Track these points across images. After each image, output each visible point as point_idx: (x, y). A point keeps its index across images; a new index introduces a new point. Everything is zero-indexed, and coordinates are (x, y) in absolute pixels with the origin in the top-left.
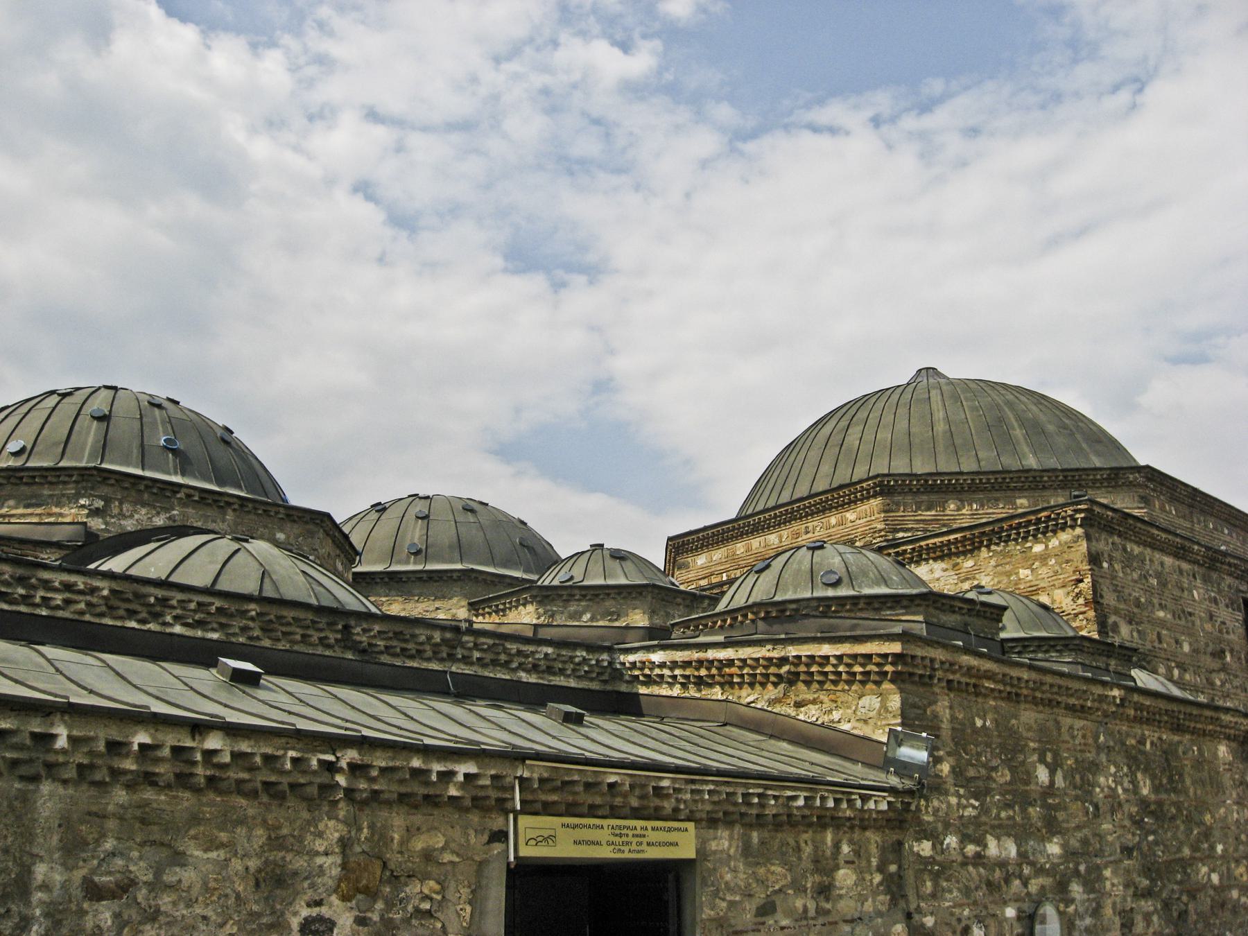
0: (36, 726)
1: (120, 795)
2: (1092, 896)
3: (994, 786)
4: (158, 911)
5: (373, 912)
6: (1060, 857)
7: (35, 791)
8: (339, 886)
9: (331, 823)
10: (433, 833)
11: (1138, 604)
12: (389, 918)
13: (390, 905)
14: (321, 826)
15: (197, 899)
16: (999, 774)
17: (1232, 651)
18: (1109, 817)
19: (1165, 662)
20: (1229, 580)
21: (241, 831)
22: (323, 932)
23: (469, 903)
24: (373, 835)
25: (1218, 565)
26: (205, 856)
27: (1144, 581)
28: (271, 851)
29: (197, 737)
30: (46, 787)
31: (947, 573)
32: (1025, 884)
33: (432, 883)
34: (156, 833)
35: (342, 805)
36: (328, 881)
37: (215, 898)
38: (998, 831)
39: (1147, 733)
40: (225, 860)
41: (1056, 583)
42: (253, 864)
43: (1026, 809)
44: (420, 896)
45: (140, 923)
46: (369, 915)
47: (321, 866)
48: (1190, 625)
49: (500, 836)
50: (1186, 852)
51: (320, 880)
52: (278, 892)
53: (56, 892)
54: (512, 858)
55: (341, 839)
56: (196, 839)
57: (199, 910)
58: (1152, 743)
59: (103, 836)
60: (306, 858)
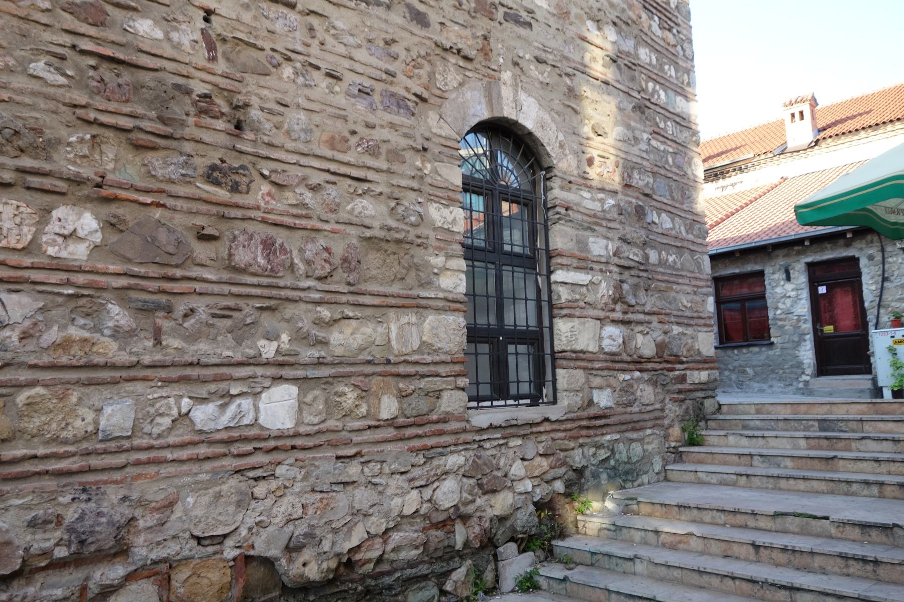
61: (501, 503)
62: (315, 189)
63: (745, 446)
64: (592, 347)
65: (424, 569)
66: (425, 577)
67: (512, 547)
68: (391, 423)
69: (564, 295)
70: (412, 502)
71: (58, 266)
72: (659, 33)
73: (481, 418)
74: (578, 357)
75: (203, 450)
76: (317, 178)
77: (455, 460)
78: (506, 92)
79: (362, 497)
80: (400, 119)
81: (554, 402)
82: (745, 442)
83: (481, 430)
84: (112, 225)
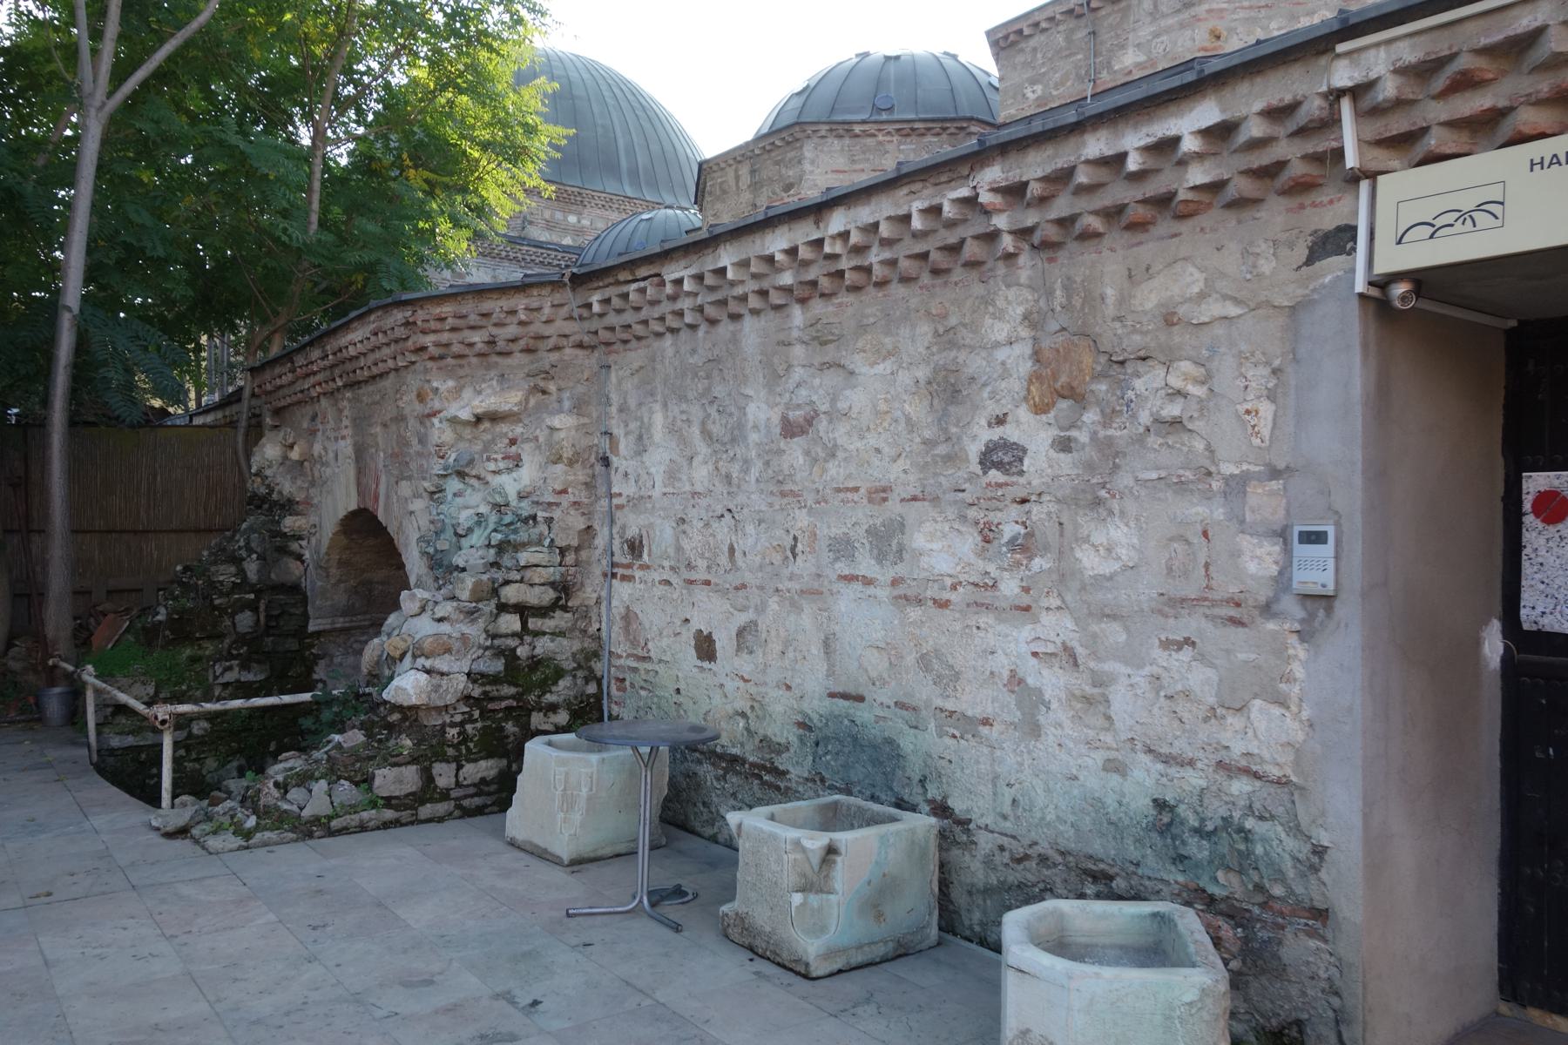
0: (708, 263)
1: (797, 315)
4: (835, 445)
5: (1080, 428)
7: (741, 330)
8: (1028, 390)
9: (1012, 293)
10: (1178, 267)
12: (1110, 438)
13: (1109, 417)
14: (1000, 303)
15: (868, 429)
21: (904, 331)
22: (1010, 463)
23: (1268, 398)
24: (1069, 298)
26: (873, 371)
28: (940, 351)
29: (821, 225)
30: (748, 322)
33: (1186, 366)
34: (830, 353)
35: (1024, 259)
36: (1016, 385)
37: (886, 424)
40: (892, 373)
42: (922, 373)
44: (1163, 392)
45: (826, 461)
46: (1074, 433)
47: (1003, 363)
49: (1339, 240)
51: (1004, 385)
52: (952, 409)
53: (763, 431)
54: (1360, 286)
55: (1026, 317)
56: (864, 351)
57: (872, 440)
59: (789, 367)
60: (984, 354)
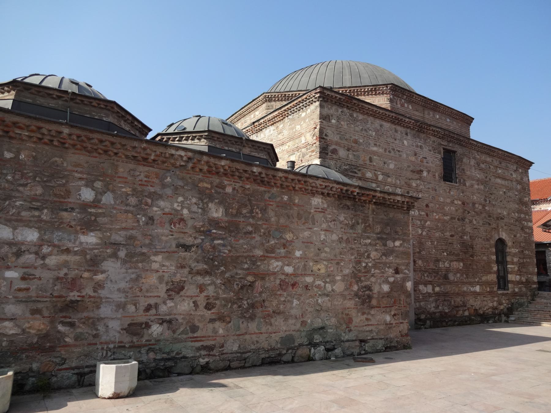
2: (130, 271)
3: (17, 195)
6: (97, 244)
11: (356, 142)
16: (28, 188)
17: (429, 172)
18: (167, 225)
19: (373, 171)
20: (433, 138)
25: (425, 130)
27: (363, 132)
31: (274, 132)
32: (44, 258)
38: (16, 223)
39: (226, 182)
41: (307, 130)
43: (58, 213)
48: (397, 156)
50: (259, 252)
58: (234, 189)
61: (502, 307)
62: (480, 256)
63: (545, 301)
64: (515, 280)
65: (492, 316)
66: (492, 317)
67: (503, 315)
68: (489, 292)
69: (510, 270)
70: (491, 305)
71: (460, 270)
72: (524, 209)
73: (500, 292)
74: (512, 282)
75: (472, 294)
76: (480, 254)
77: (496, 299)
78: (501, 233)
79: (485, 303)
80: (488, 242)
81: (508, 290)
82: (545, 301)
83: (499, 294)
84: (464, 264)
